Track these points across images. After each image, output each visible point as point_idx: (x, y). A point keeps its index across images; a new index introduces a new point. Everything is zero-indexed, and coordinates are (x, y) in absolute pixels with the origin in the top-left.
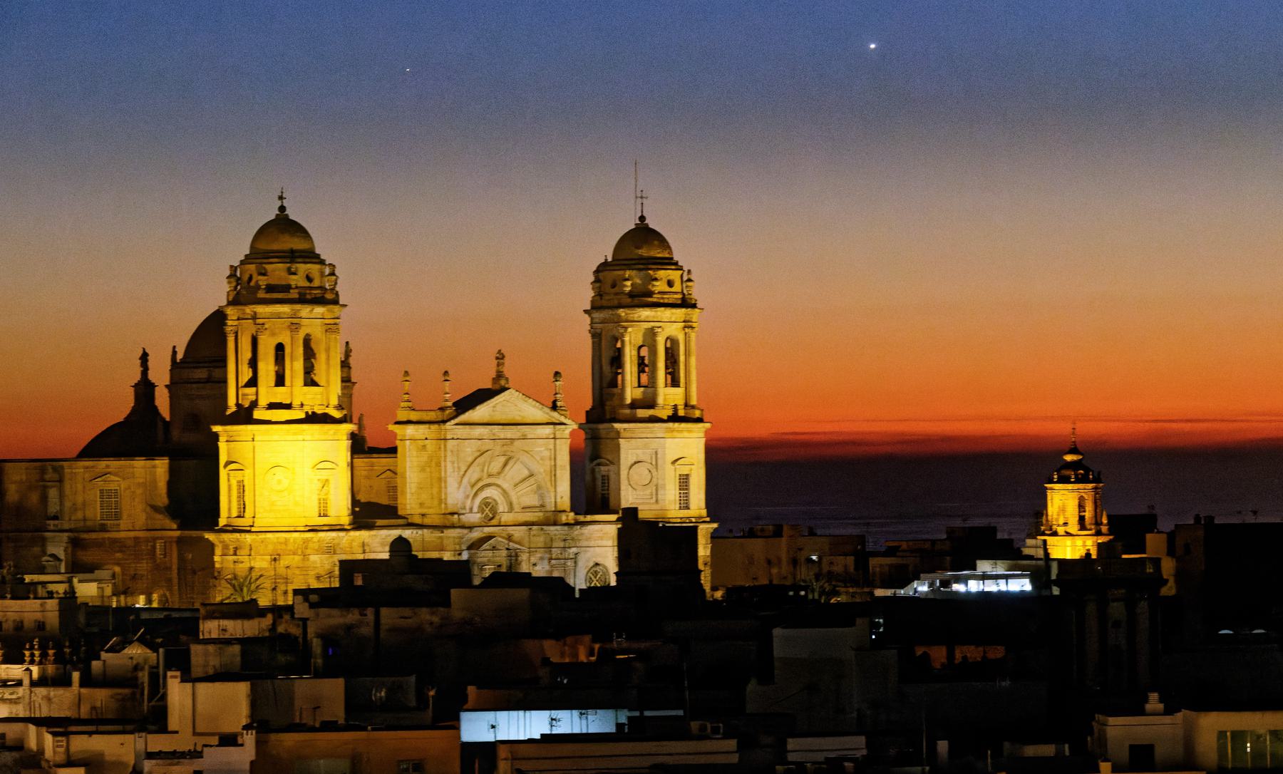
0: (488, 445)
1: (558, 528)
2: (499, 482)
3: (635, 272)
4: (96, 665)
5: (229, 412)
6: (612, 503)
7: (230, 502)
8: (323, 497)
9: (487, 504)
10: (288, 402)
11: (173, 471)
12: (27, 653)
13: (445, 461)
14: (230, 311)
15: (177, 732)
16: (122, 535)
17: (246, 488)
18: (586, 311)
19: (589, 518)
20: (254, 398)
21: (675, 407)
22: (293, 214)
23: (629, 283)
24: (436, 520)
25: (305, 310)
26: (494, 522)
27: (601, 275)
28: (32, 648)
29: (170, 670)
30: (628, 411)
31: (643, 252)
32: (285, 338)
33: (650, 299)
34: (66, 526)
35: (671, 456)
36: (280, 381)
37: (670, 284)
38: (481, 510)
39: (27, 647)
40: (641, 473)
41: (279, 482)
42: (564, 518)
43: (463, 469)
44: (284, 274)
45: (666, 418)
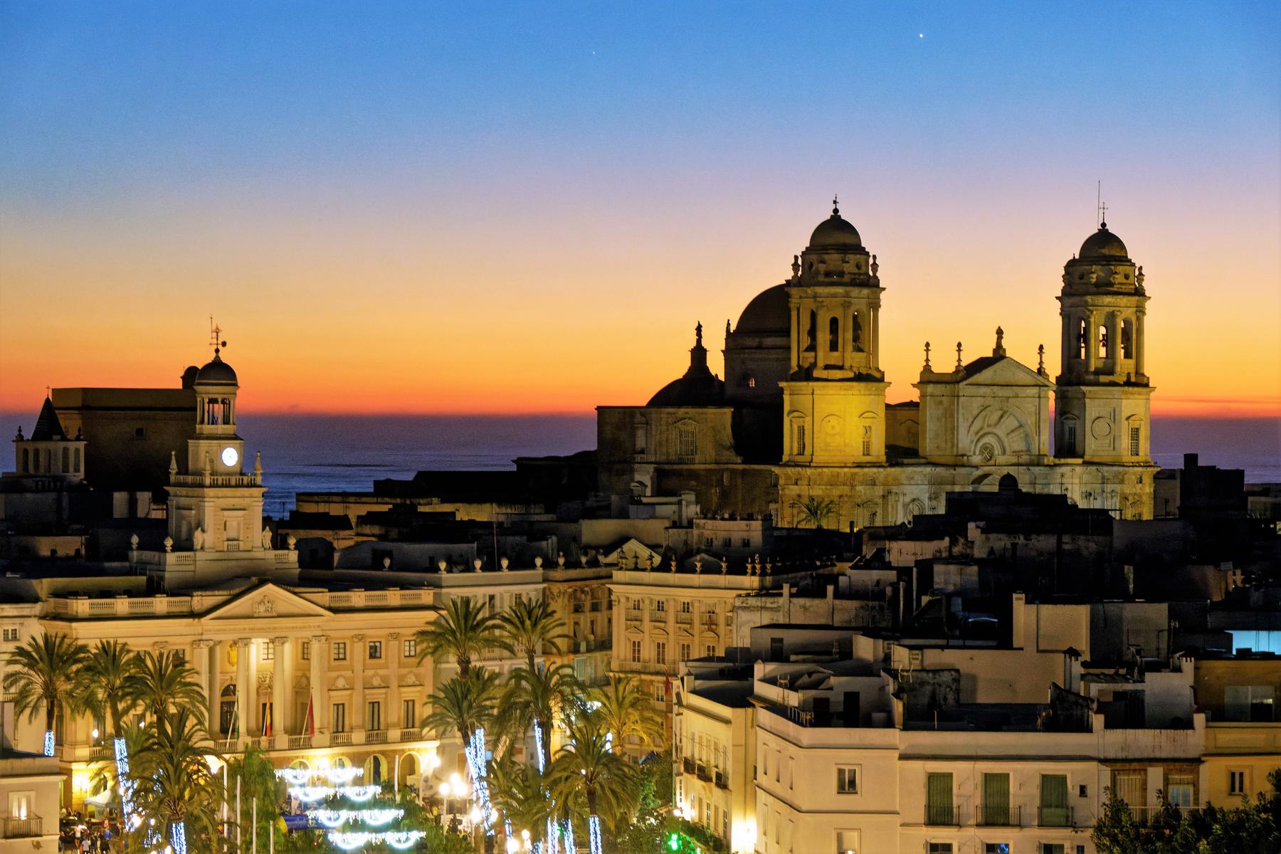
0: (989, 401)
1: (1042, 468)
2: (996, 431)
3: (1099, 267)
5: (792, 372)
6: (1078, 449)
8: (866, 440)
10: (841, 364)
11: (734, 415)
12: (749, 566)
13: (958, 414)
14: (794, 291)
15: (1022, 649)
16: (697, 467)
17: (806, 433)
18: (1057, 298)
19: (1063, 461)
20: (813, 360)
21: (1129, 374)
22: (844, 215)
23: (1094, 276)
24: (951, 460)
25: (855, 292)
26: (992, 462)
27: (1071, 270)
28: (753, 562)
29: (1015, 592)
31: (1106, 251)
32: (838, 314)
33: (1111, 289)
35: (1125, 414)
37: (1127, 277)
38: (981, 453)
39: (750, 561)
40: (1101, 427)
41: (833, 427)
42: (1046, 461)
43: (971, 420)
45: (1122, 383)
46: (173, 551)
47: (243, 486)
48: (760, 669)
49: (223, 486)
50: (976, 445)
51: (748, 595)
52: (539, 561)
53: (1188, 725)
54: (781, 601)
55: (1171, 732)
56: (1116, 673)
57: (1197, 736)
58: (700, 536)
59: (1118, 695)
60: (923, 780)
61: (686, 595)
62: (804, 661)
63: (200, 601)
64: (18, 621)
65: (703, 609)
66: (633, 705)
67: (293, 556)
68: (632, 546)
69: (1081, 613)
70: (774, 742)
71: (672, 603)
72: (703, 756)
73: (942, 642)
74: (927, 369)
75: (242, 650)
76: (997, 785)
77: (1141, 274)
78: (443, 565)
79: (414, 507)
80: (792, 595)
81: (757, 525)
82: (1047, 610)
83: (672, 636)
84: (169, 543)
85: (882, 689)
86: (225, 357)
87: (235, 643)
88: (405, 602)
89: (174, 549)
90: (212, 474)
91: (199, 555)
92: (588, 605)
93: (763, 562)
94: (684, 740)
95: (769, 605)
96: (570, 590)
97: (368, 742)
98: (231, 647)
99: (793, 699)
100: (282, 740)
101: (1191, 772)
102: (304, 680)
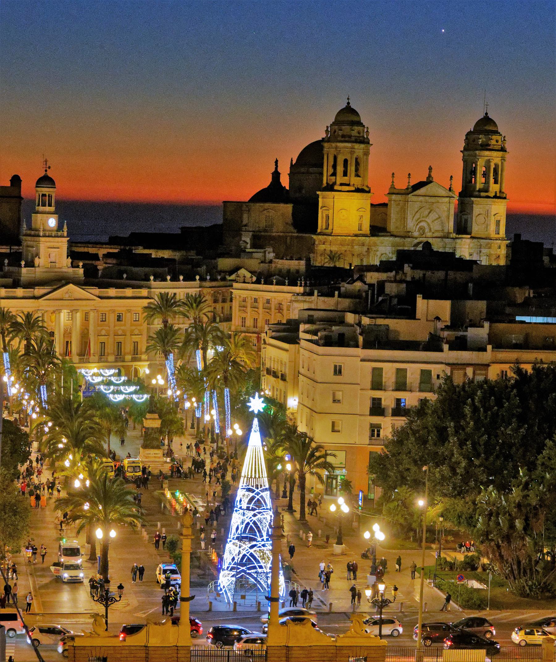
2: (427, 220)
4: (343, 289)
5: (323, 186)
6: (468, 229)
7: (322, 222)
9: (421, 229)
12: (299, 282)
14: (326, 145)
15: (420, 319)
16: (274, 234)
18: (461, 151)
19: (460, 236)
20: (334, 181)
21: (496, 192)
22: (353, 106)
23: (481, 140)
24: (402, 234)
25: (356, 146)
26: (424, 236)
28: (301, 280)
30: (477, 193)
33: (489, 147)
35: (493, 213)
36: (345, 174)
37: (497, 141)
38: (419, 231)
40: (481, 219)
42: (451, 236)
43: (414, 214)
46: (25, 267)
47: (58, 237)
48: (302, 327)
49: (48, 236)
50: (416, 227)
52: (198, 277)
53: (485, 350)
55: (476, 352)
57: (488, 355)
59: (457, 338)
61: (268, 295)
63: (39, 291)
66: (243, 345)
67: (81, 271)
68: (242, 272)
70: (306, 353)
71: (261, 299)
72: (275, 367)
74: (393, 187)
75: (57, 315)
76: (402, 374)
78: (152, 278)
79: (132, 250)
80: (318, 296)
81: (303, 262)
82: (432, 302)
83: (261, 316)
84: (23, 263)
85: (355, 332)
86: (50, 174)
87: (54, 312)
88: (134, 295)
89: (26, 266)
90: (43, 231)
91: (37, 269)
92: (220, 300)
93: (305, 280)
94: (267, 359)
95: (307, 300)
96: (212, 292)
97: (116, 361)
98: (52, 313)
99: (315, 338)
100: (76, 359)
101: (485, 370)
102: (86, 330)
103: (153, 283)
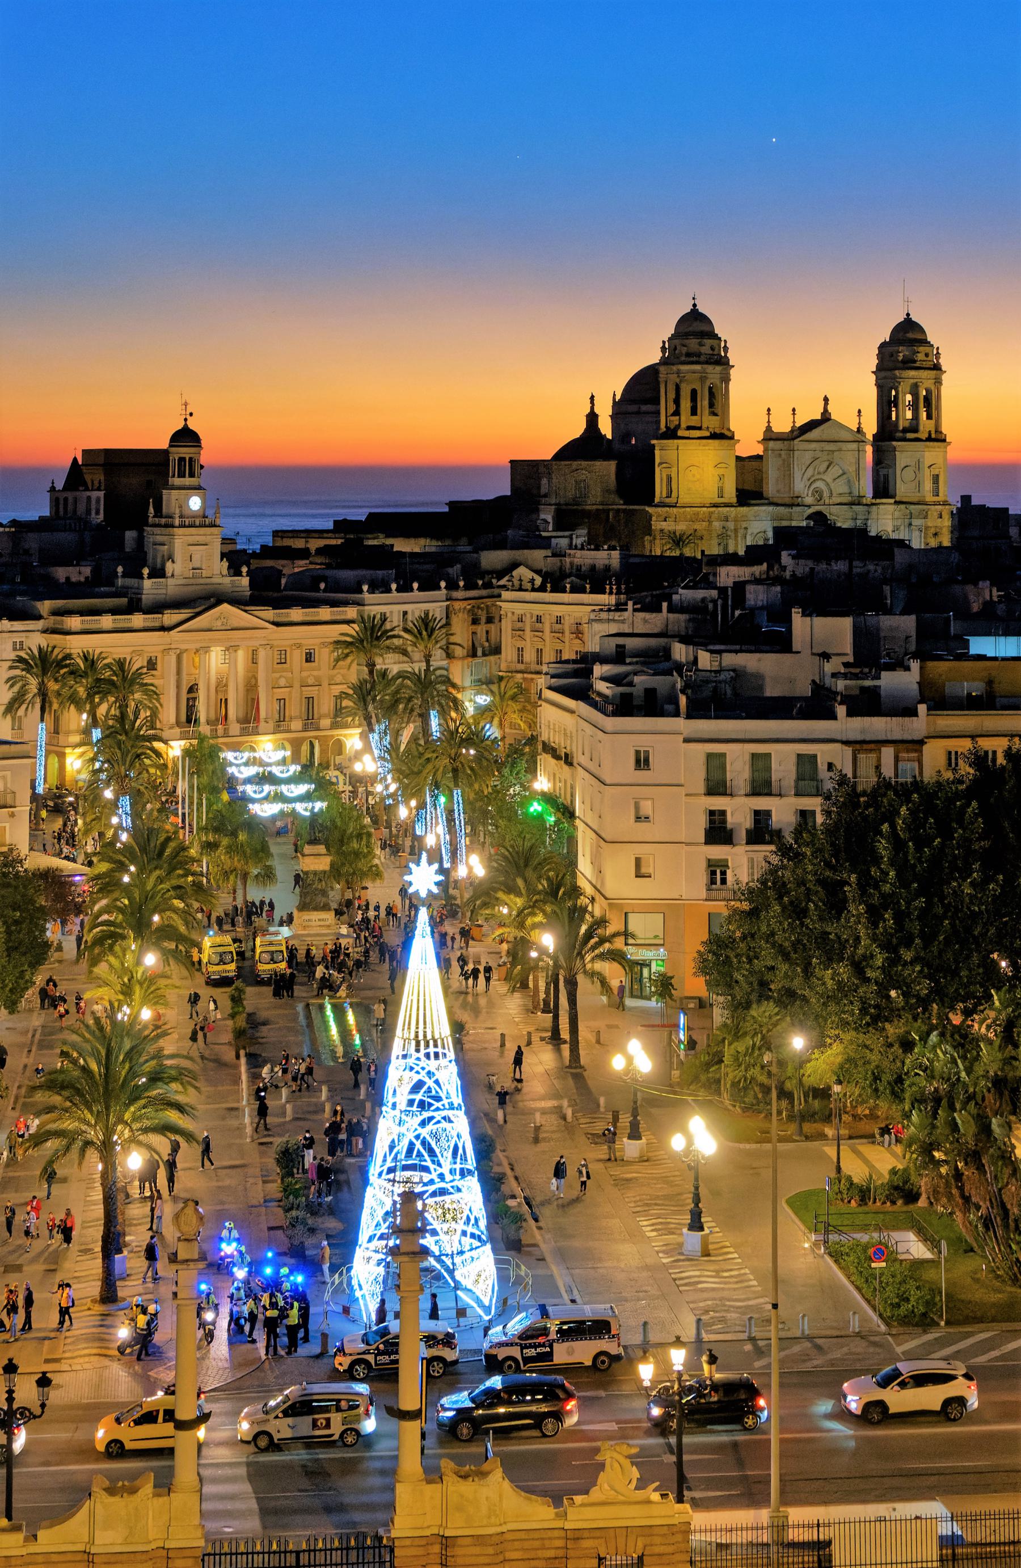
0: (818, 454)
2: (824, 477)
4: (675, 597)
6: (891, 492)
12: (608, 587)
14: (662, 369)
16: (588, 507)
19: (878, 501)
21: (930, 433)
22: (701, 309)
23: (901, 355)
24: (787, 501)
25: (710, 368)
26: (822, 502)
27: (884, 350)
28: (611, 584)
30: (901, 434)
31: (910, 335)
32: (697, 386)
34: (553, 502)
35: (927, 463)
37: (927, 355)
38: (813, 495)
40: (909, 474)
41: (694, 476)
42: (864, 501)
44: (697, 346)
47: (205, 526)
48: (599, 670)
51: (601, 610)
52: (443, 584)
53: (914, 713)
54: (626, 614)
56: (861, 672)
57: (921, 723)
58: (572, 564)
59: (863, 689)
60: (702, 759)
61: (558, 610)
62: (637, 663)
63: (170, 617)
64: (24, 634)
65: (572, 621)
66: (513, 698)
67: (245, 581)
69: (845, 625)
70: (589, 729)
71: (548, 617)
72: (556, 740)
73: (738, 647)
74: (769, 428)
75: (202, 656)
76: (760, 763)
77: (938, 353)
78: (365, 588)
79: (362, 540)
80: (635, 610)
81: (616, 554)
82: (819, 622)
84: (146, 571)
85: (674, 686)
86: (192, 425)
87: (197, 651)
89: (150, 577)
90: (181, 517)
92: (483, 619)
95: (616, 618)
96: (469, 607)
97: (305, 730)
100: (235, 728)
101: (916, 751)
103: (367, 596)
